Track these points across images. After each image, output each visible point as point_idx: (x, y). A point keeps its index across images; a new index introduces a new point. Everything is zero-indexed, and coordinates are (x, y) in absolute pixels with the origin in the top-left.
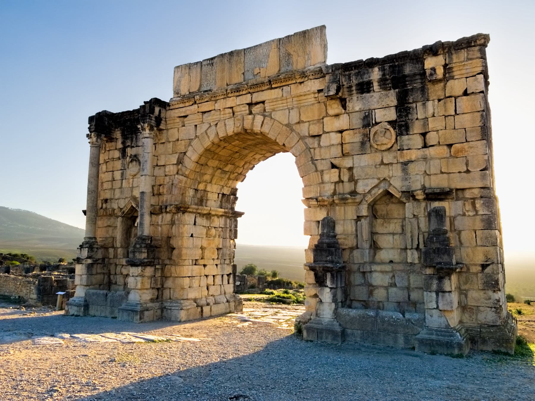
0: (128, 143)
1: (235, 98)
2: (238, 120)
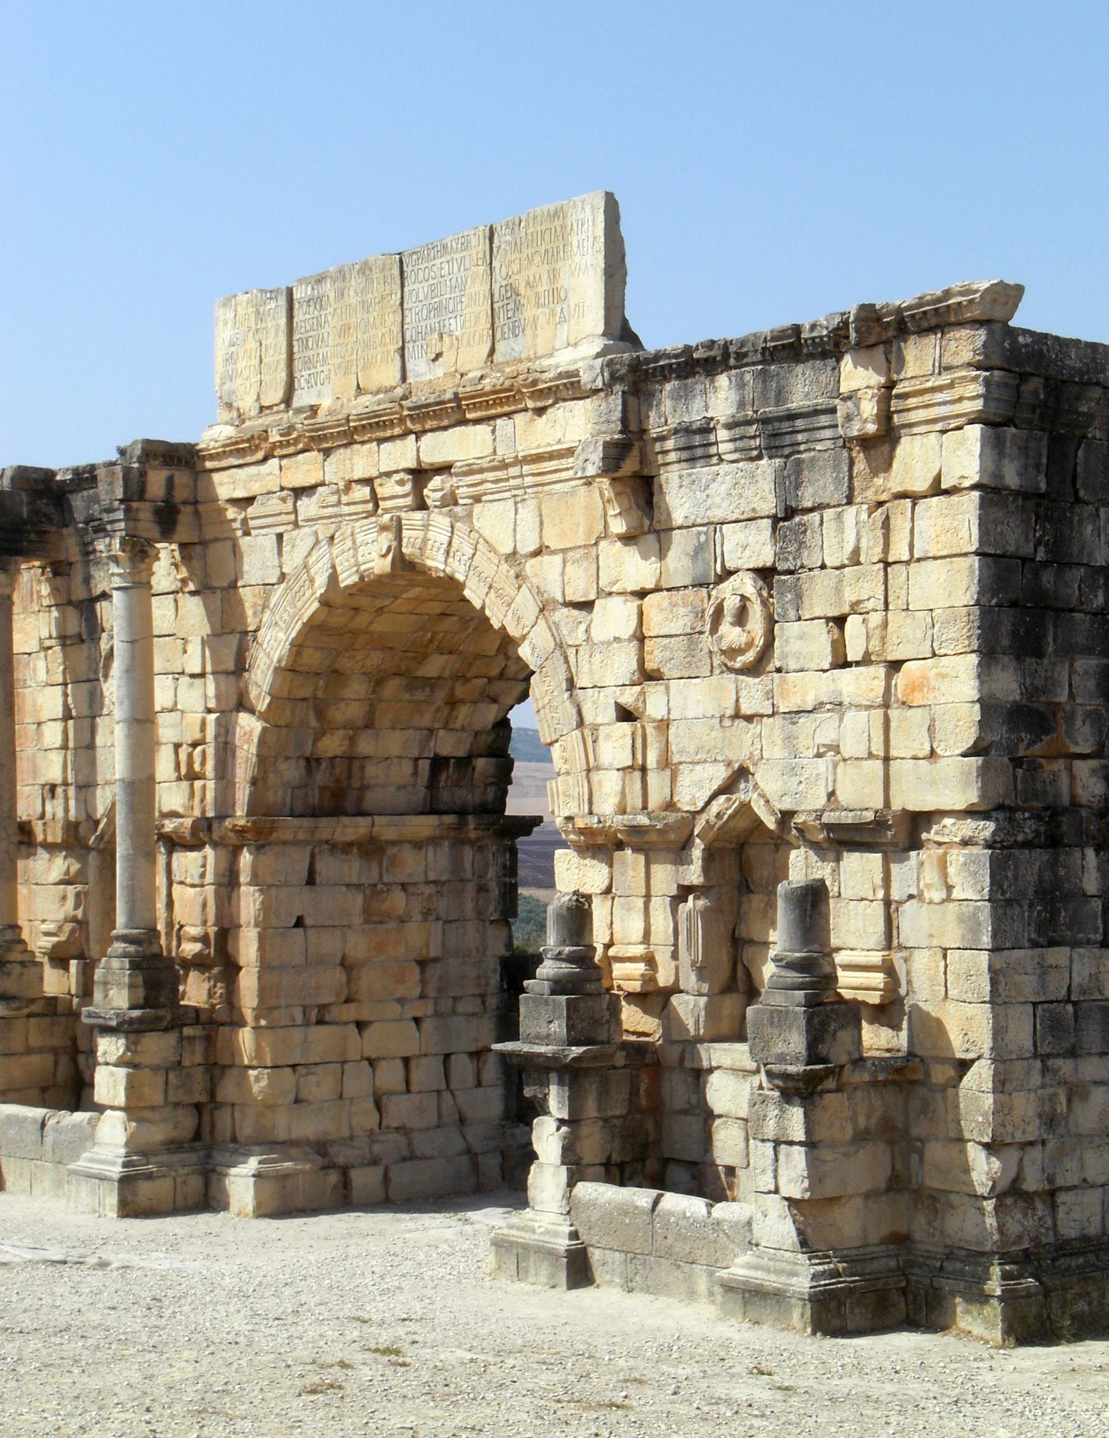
2: (384, 528)
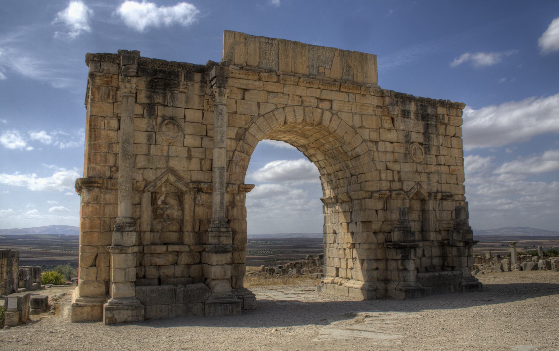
0: (159, 99)
1: (305, 88)
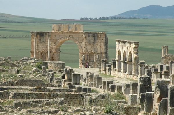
0: (41, 38)
